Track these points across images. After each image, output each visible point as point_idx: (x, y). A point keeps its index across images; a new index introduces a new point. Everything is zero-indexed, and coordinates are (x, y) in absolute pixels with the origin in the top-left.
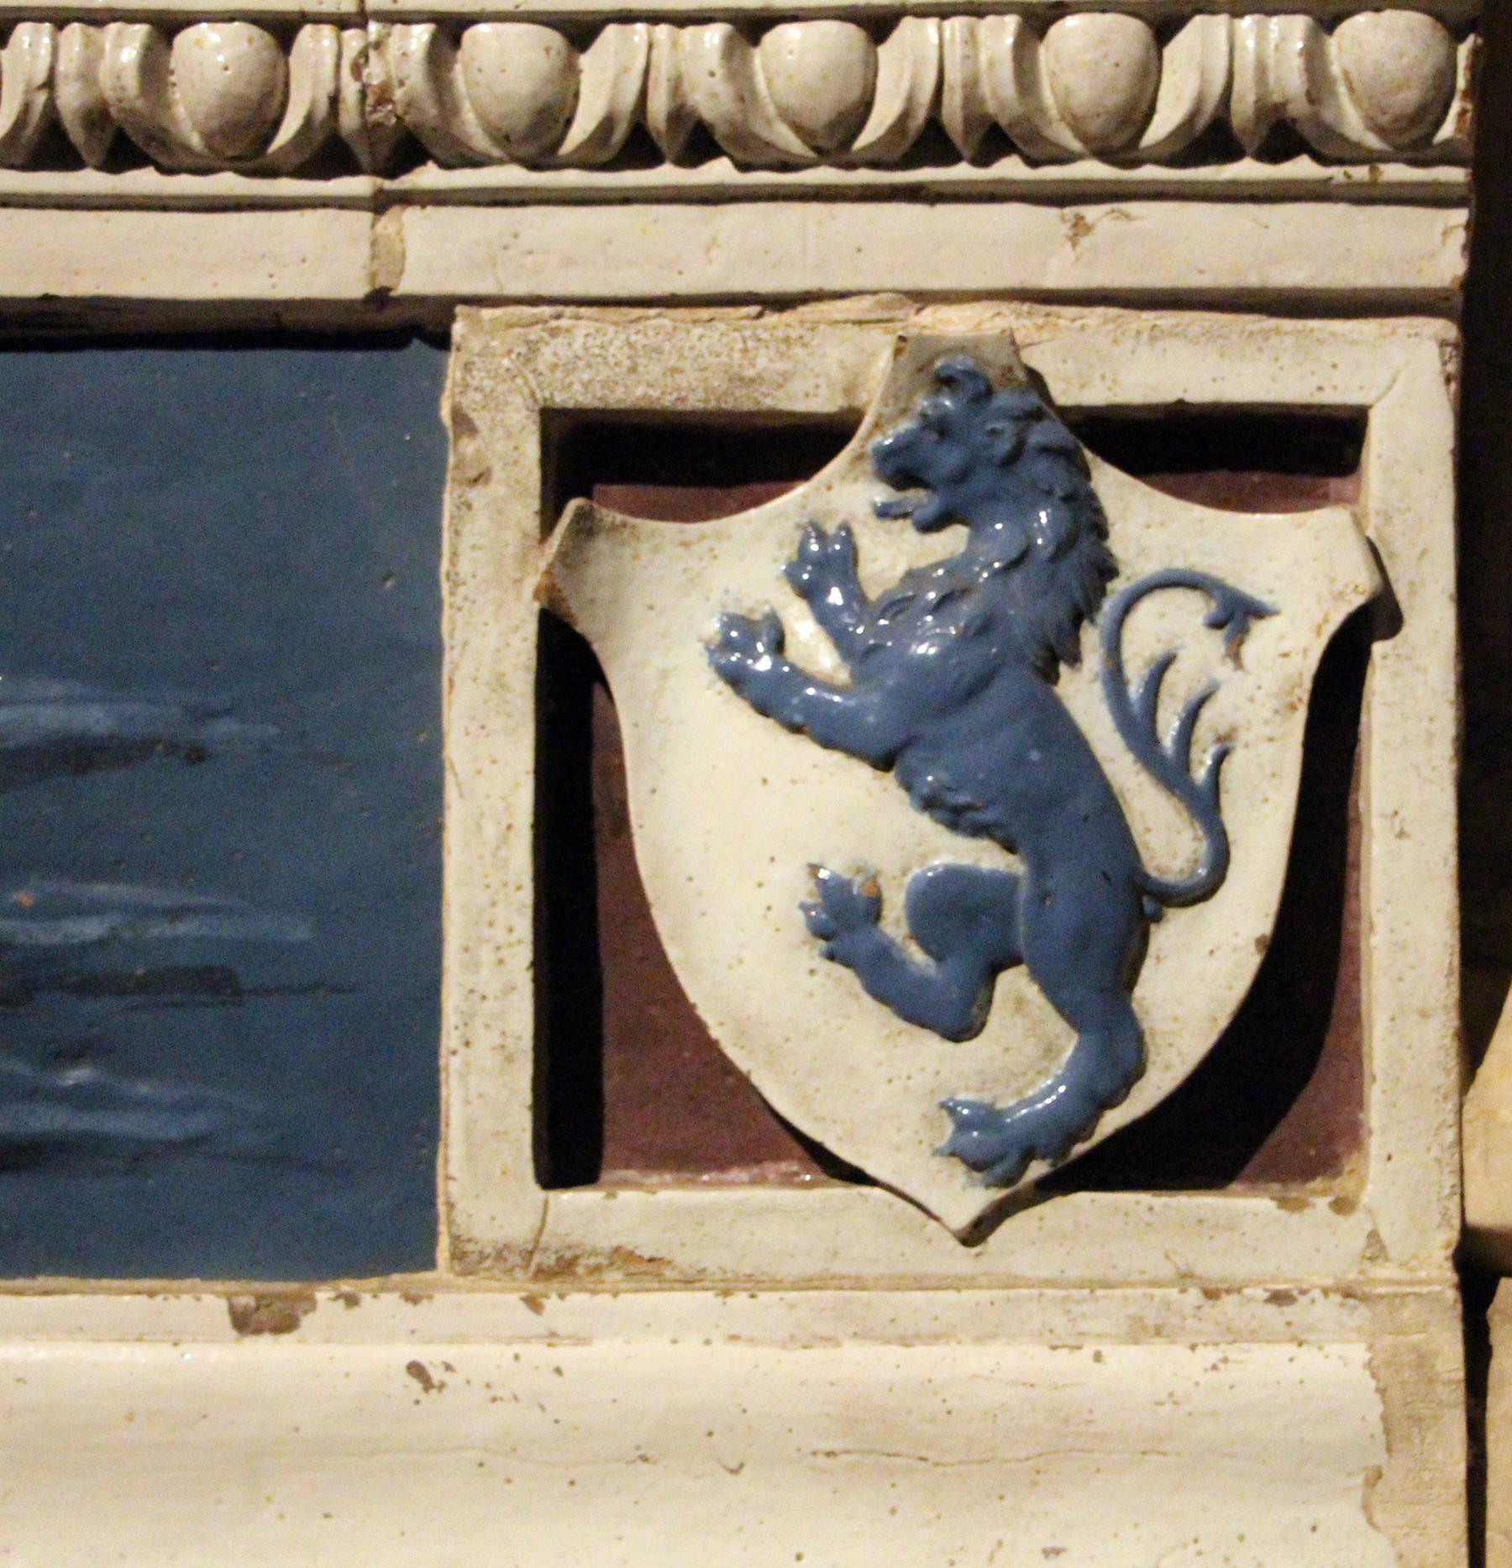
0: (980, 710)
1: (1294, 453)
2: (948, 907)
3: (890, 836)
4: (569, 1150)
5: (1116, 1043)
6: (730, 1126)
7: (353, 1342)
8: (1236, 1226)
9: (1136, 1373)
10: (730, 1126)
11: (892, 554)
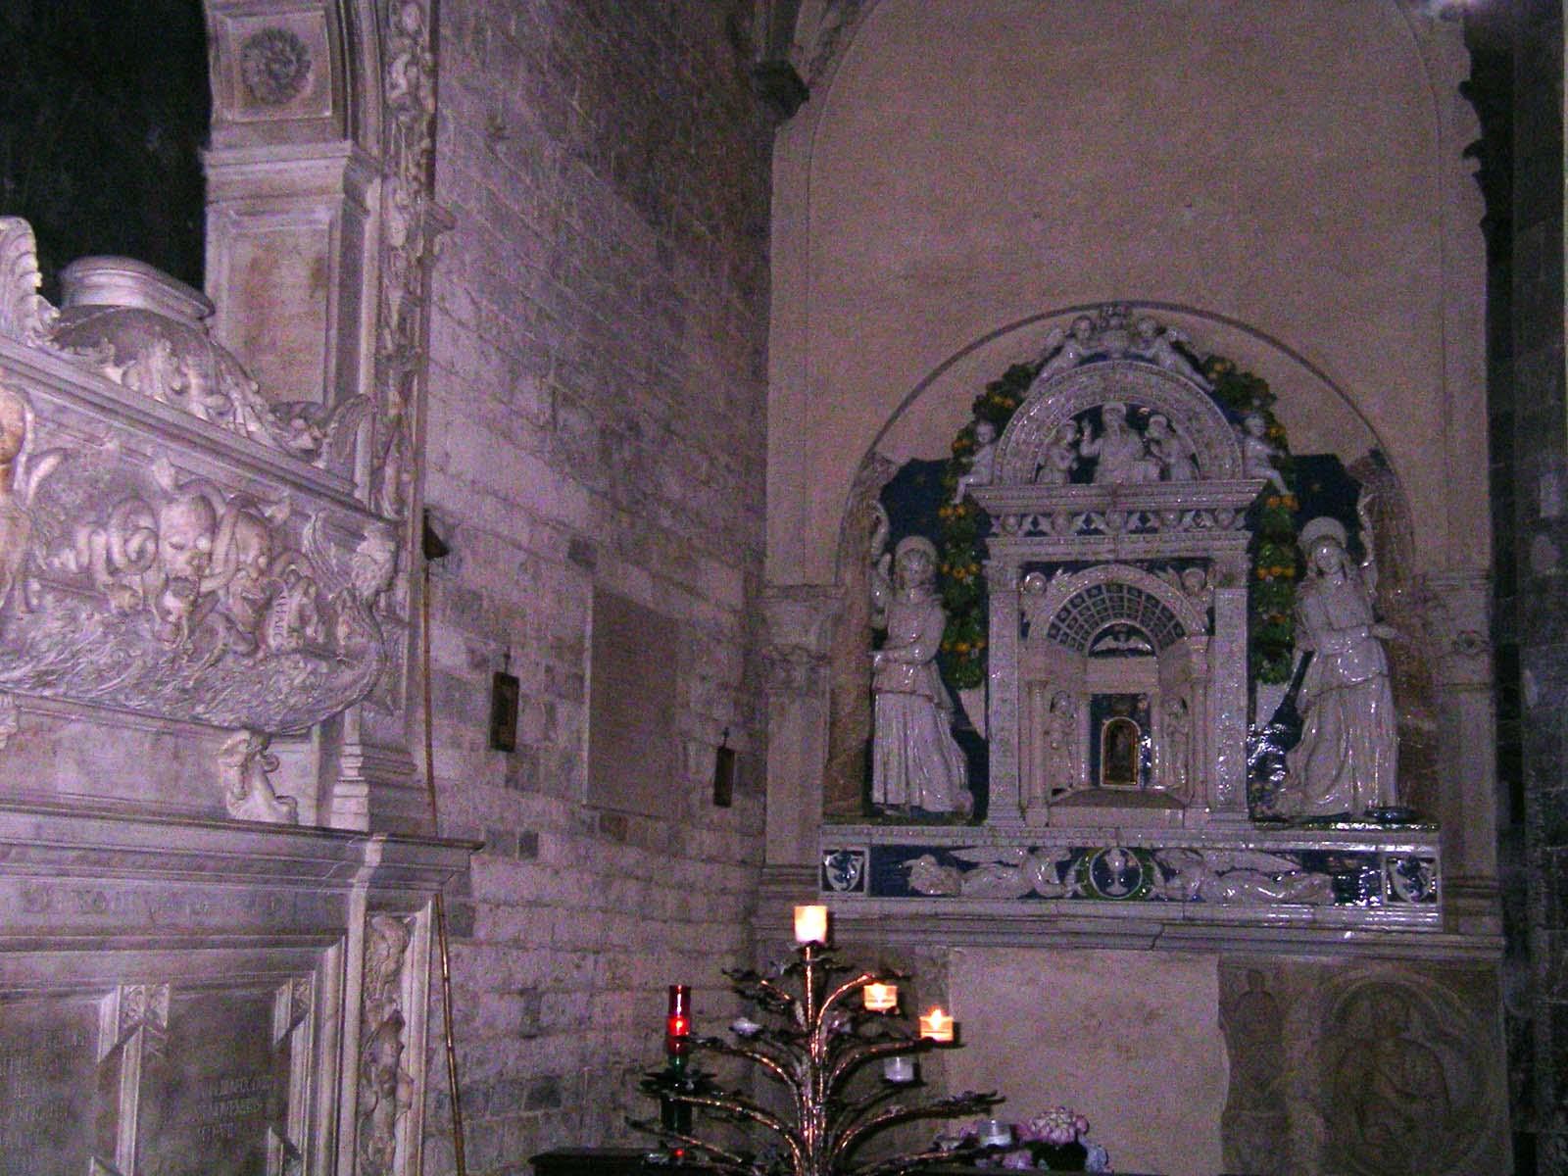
5: (1421, 893)
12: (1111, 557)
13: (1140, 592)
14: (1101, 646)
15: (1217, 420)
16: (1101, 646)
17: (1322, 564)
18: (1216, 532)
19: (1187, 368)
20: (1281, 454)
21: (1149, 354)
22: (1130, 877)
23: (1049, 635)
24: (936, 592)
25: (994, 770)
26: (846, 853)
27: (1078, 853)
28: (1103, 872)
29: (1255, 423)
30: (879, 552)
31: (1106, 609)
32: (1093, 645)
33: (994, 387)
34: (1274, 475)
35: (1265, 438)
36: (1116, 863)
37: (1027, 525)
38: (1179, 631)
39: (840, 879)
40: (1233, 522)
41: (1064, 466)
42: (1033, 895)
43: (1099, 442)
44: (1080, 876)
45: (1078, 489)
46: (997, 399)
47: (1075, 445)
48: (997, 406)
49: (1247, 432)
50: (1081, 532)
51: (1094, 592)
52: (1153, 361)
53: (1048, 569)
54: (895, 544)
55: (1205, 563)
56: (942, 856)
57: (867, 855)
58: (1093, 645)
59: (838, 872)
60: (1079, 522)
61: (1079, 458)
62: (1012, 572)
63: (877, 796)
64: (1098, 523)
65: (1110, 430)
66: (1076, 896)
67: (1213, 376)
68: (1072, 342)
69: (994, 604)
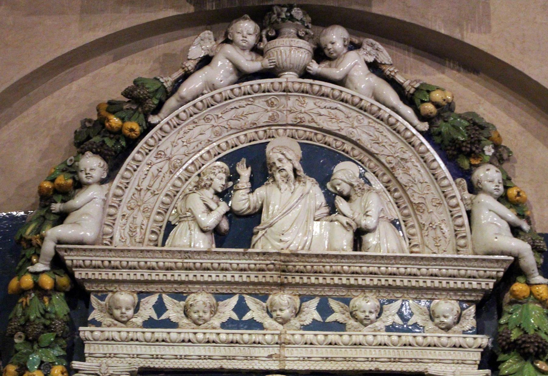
18: (433, 335)
19: (392, 97)
20: (525, 226)
21: (336, 72)
29: (488, 175)
33: (113, 107)
34: (521, 246)
35: (503, 199)
37: (148, 310)
40: (459, 318)
43: (260, 191)
45: (232, 258)
46: (115, 121)
47: (224, 195)
48: (112, 138)
49: (473, 189)
50: (228, 324)
52: (341, 82)
61: (231, 214)
65: (278, 176)
67: (429, 108)
68: (229, 49)
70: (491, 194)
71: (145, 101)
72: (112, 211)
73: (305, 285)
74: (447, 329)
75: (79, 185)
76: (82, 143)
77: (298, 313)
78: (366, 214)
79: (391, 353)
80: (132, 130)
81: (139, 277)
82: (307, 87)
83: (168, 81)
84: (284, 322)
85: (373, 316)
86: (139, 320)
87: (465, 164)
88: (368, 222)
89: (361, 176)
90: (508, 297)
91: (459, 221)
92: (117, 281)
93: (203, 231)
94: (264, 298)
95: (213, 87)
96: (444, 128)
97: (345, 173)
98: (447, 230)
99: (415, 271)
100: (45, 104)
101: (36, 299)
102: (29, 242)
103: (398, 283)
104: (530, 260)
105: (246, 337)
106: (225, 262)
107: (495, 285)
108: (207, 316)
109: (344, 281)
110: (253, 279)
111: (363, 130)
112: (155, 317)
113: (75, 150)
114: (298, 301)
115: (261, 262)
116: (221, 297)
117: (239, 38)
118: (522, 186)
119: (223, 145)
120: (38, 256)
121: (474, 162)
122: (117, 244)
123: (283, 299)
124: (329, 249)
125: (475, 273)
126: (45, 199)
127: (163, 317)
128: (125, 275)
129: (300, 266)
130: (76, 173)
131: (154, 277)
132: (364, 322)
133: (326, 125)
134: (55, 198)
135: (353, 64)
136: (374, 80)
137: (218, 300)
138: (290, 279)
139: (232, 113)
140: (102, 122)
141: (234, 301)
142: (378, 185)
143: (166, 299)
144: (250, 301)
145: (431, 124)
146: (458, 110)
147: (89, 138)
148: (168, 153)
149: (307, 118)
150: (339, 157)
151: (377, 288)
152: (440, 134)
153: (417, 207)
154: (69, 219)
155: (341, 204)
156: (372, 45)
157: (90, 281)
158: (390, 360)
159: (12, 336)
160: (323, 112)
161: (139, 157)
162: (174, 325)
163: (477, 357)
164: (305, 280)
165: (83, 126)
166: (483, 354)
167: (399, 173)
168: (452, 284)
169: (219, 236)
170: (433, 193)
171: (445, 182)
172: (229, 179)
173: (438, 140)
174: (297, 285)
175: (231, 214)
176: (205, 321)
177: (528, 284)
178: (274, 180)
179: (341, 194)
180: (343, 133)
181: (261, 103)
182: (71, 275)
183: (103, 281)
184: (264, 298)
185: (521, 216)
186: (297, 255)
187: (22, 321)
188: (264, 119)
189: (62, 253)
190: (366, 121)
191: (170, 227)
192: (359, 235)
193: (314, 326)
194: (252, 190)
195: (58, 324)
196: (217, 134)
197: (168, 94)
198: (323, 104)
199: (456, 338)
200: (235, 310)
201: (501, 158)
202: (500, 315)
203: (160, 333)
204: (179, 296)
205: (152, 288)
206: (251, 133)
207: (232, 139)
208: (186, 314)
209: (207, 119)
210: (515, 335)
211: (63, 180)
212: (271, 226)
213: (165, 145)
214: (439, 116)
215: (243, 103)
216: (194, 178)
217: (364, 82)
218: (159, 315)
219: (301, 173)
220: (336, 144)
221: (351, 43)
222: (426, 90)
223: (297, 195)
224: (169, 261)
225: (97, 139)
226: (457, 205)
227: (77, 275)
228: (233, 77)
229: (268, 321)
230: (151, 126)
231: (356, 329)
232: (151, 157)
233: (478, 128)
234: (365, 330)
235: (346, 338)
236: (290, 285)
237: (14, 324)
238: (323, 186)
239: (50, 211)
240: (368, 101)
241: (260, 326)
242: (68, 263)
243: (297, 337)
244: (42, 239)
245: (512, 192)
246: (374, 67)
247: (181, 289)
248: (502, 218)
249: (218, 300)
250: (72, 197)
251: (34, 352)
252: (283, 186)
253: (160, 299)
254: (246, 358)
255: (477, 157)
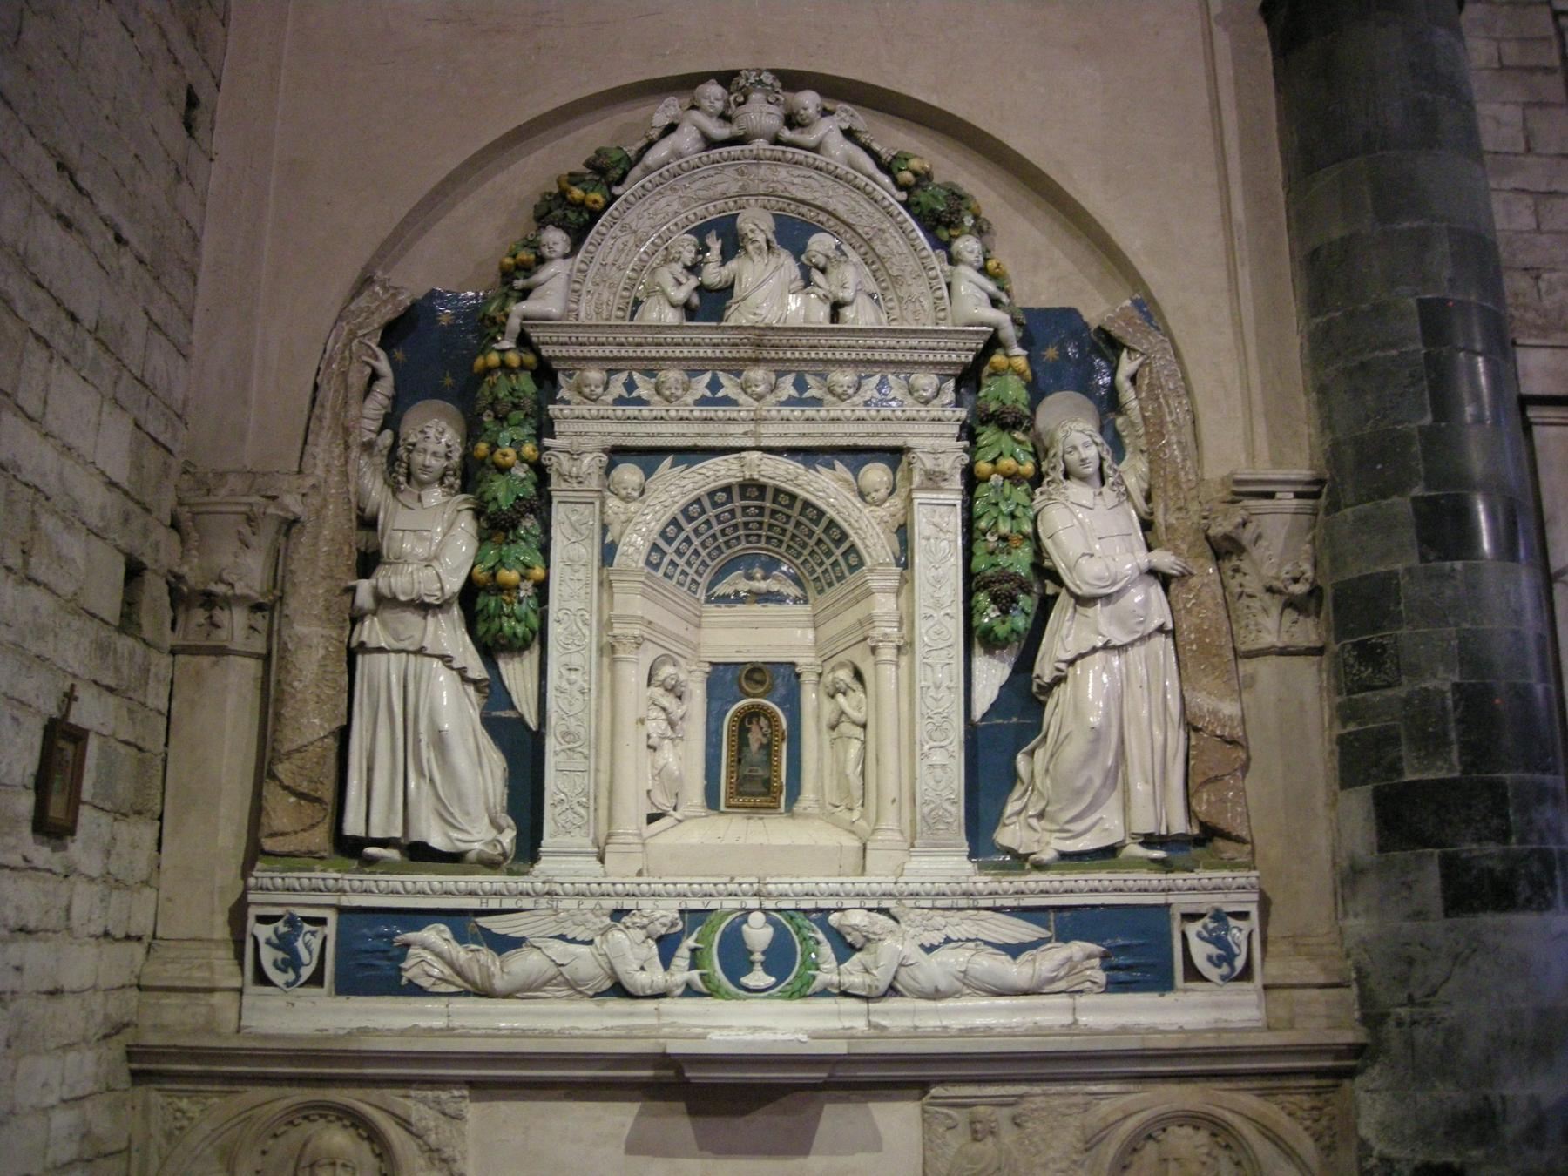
0: (1219, 941)
1: (1244, 916)
2: (1219, 957)
3: (1213, 950)
4: (1186, 979)
6: (1201, 977)
7: (1169, 998)
8: (1245, 985)
9: (1237, 998)
10: (1201, 977)
11: (1211, 925)
12: (750, 443)
13: (793, 497)
14: (721, 589)
15: (912, 243)
16: (721, 589)
17: (1073, 458)
18: (913, 409)
19: (868, 164)
20: (1005, 299)
21: (810, 138)
22: (780, 958)
23: (648, 563)
24: (463, 490)
25: (554, 783)
26: (292, 921)
27: (695, 918)
28: (736, 957)
29: (968, 246)
30: (374, 426)
31: (735, 527)
32: (712, 584)
33: (575, 179)
34: (1001, 317)
35: (983, 270)
36: (758, 934)
37: (617, 389)
38: (853, 560)
39: (282, 967)
41: (680, 295)
42: (619, 990)
43: (733, 265)
44: (695, 961)
46: (577, 193)
47: (694, 269)
48: (574, 212)
50: (703, 401)
51: (721, 497)
53: (649, 456)
54: (399, 420)
55: (894, 455)
56: (459, 921)
57: (331, 930)
58: (712, 584)
59: (281, 955)
60: (701, 385)
62: (591, 463)
63: (353, 825)
64: (729, 388)
65: (750, 247)
66: (690, 991)
67: (906, 176)
68: (695, 114)
69: (559, 513)
70: (971, 265)
71: (608, 172)
72: (577, 286)
73: (781, 360)
74: (927, 402)
75: (541, 260)
76: (542, 219)
77: (773, 388)
78: (843, 287)
79: (872, 429)
80: (596, 202)
81: (608, 354)
82: (780, 155)
83: (632, 151)
84: (760, 398)
85: (851, 391)
86: (609, 399)
87: (944, 234)
88: (847, 295)
89: (838, 247)
90: (987, 370)
91: (939, 293)
92: (585, 359)
93: (673, 305)
94: (738, 374)
95: (680, 156)
96: (922, 197)
97: (820, 244)
98: (927, 303)
99: (893, 343)
100: (501, 178)
101: (503, 378)
102: (493, 320)
103: (877, 357)
104: (1009, 332)
105: (720, 414)
106: (697, 337)
107: (976, 358)
108: (679, 393)
109: (821, 355)
110: (726, 354)
111: (840, 200)
112: (625, 394)
113: (534, 225)
114: (773, 377)
115: (735, 337)
116: (693, 373)
117: (706, 103)
118: (1001, 258)
119: (692, 217)
120: (503, 333)
121: (953, 233)
122: (583, 319)
123: (758, 374)
124: (806, 319)
125: (954, 345)
126: (507, 275)
127: (634, 395)
128: (593, 352)
129: (775, 340)
130: (537, 248)
131: (623, 354)
132: (841, 397)
133: (800, 196)
134: (517, 275)
135: (827, 130)
136: (850, 147)
137: (690, 377)
138: (765, 354)
139: (700, 184)
140: (563, 194)
141: (707, 378)
142: (854, 257)
143: (636, 376)
144: (723, 378)
145: (909, 194)
146: (936, 180)
147: (550, 211)
148: (633, 225)
149: (780, 187)
150: (813, 229)
151: (856, 363)
152: (918, 204)
153: (895, 280)
154: (533, 295)
155: (817, 276)
156: (846, 111)
157: (557, 358)
158: (869, 435)
159: (480, 414)
160: (796, 180)
161: (603, 230)
162: (644, 403)
163: (956, 430)
164: (781, 355)
165: (544, 199)
166: (962, 428)
167: (877, 245)
168: (931, 358)
169: (689, 310)
170: (912, 264)
171: (924, 254)
172: (698, 253)
173: (917, 211)
174: (773, 360)
175: (701, 289)
176: (678, 398)
177: (1007, 355)
178: (747, 252)
179: (816, 266)
180: (818, 203)
181: (731, 172)
182: (537, 353)
183: (570, 358)
184: (738, 374)
185: (1001, 289)
186: (772, 328)
187: (490, 400)
188: (734, 189)
189: (528, 330)
190: (841, 191)
191: (638, 303)
192: (836, 307)
193: (790, 402)
194: (723, 263)
195: (527, 403)
196: (685, 205)
197: (632, 165)
198: (797, 172)
199: (935, 411)
200: (709, 386)
201: (980, 230)
202: (978, 387)
203: (632, 410)
204: (650, 373)
205: (621, 365)
206: (720, 204)
207: (700, 210)
208: (658, 393)
209: (674, 190)
210: (993, 407)
211: (526, 255)
212: (744, 299)
213: (630, 217)
214: (917, 185)
215: (712, 172)
216: (661, 253)
217: (839, 148)
218: (630, 392)
219: (775, 244)
220: (811, 214)
221: (825, 109)
222: (902, 157)
223: (772, 267)
224: (639, 337)
225: (558, 212)
226: (936, 277)
227: (544, 353)
228: (701, 145)
229: (742, 398)
230: (615, 198)
231: (834, 404)
232: (616, 230)
233: (957, 197)
234: (843, 406)
235: (823, 413)
236: (765, 360)
237: (483, 403)
238: (797, 259)
239: (512, 288)
240: (843, 169)
241: (734, 403)
242: (535, 339)
243: (774, 413)
244: (507, 316)
245: (991, 264)
246: (849, 134)
247: (652, 366)
248: (982, 289)
249: (690, 377)
250: (536, 273)
251: (504, 429)
252: (756, 258)
253: (630, 376)
254: (721, 435)
255: (956, 227)
